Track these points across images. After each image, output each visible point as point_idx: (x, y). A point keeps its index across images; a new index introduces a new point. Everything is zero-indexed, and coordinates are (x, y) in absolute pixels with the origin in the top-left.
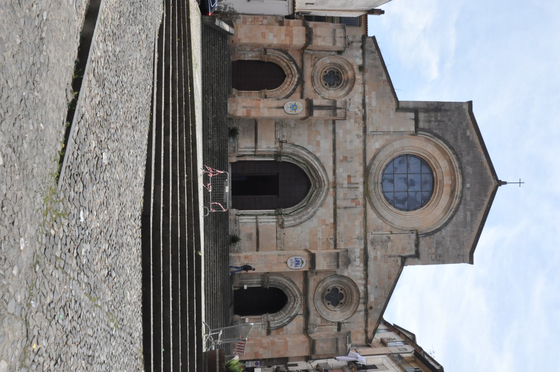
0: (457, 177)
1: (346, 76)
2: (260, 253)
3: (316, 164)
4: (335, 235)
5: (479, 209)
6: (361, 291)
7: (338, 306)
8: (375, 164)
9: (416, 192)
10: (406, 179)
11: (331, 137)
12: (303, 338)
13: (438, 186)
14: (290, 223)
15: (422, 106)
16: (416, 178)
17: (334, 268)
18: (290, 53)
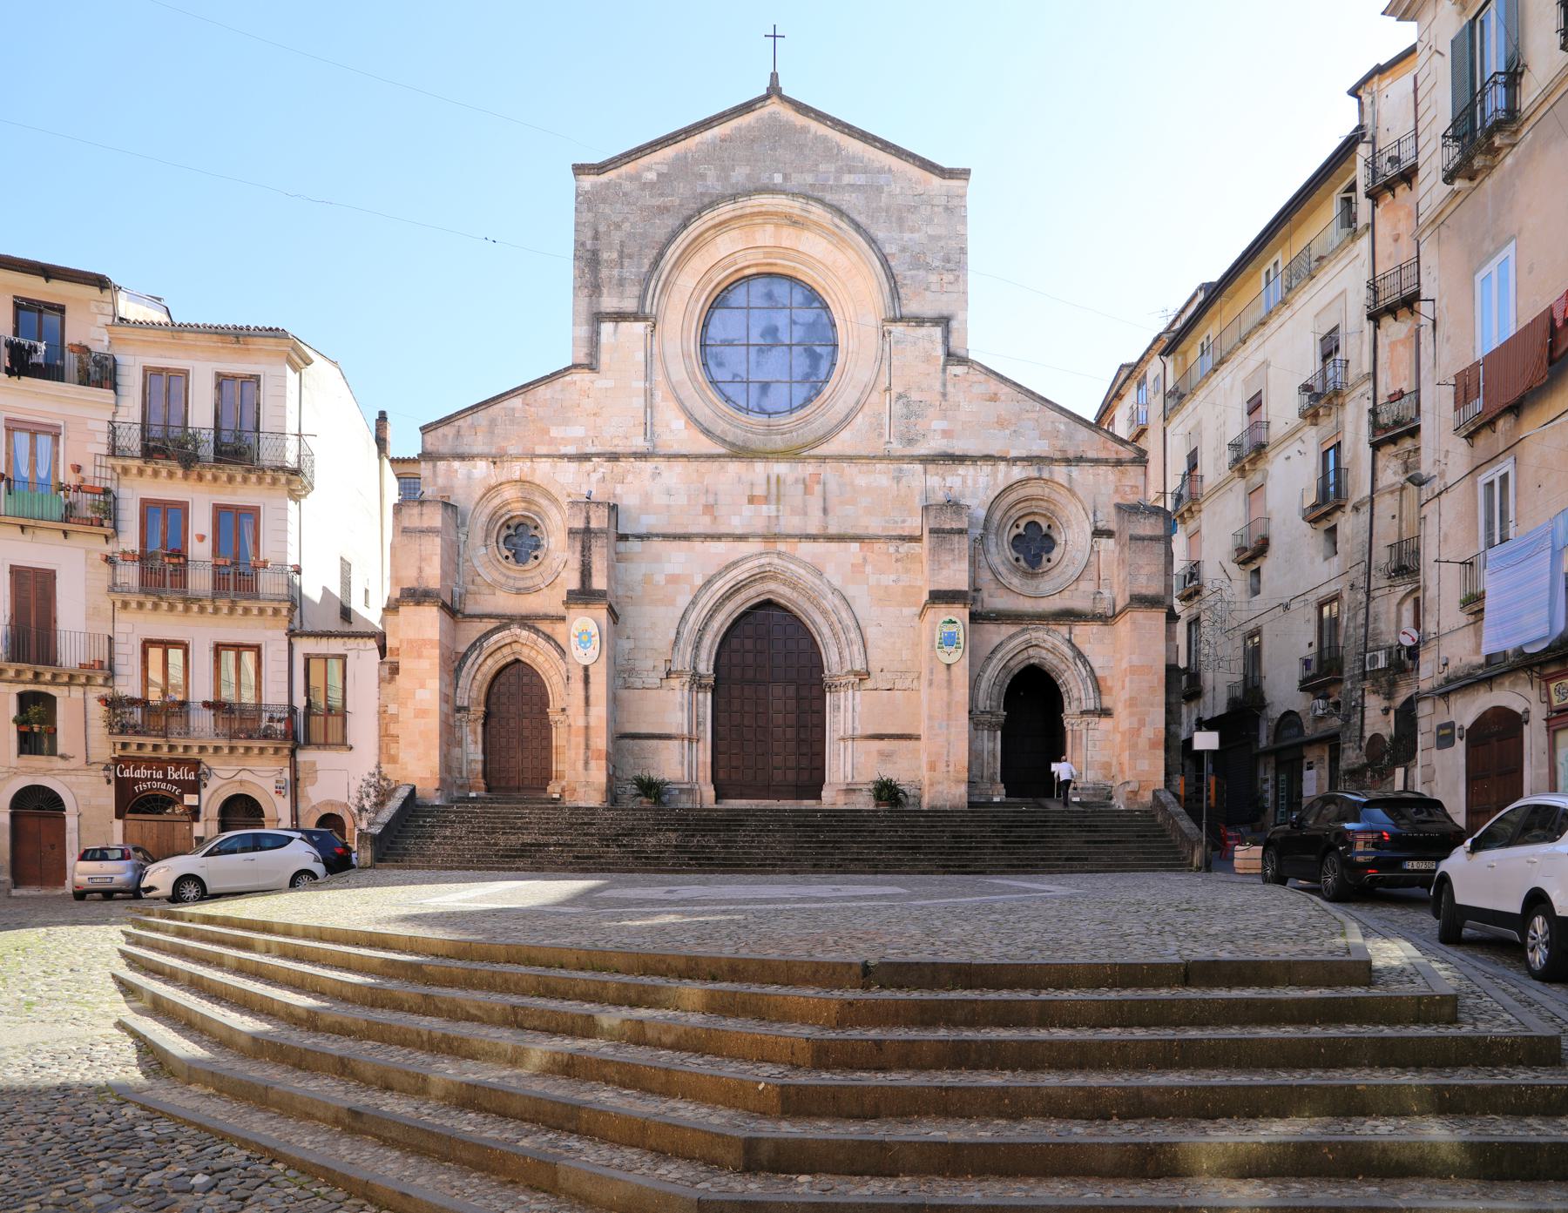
0: (756, 210)
1: (514, 505)
2: (922, 730)
3: (721, 586)
4: (890, 538)
5: (835, 151)
6: (1024, 475)
7: (1055, 535)
8: (723, 431)
9: (793, 322)
10: (762, 349)
11: (657, 545)
12: (1123, 626)
13: (779, 261)
14: (856, 652)
15: (584, 302)
16: (759, 322)
17: (963, 544)
18: (463, 649)
